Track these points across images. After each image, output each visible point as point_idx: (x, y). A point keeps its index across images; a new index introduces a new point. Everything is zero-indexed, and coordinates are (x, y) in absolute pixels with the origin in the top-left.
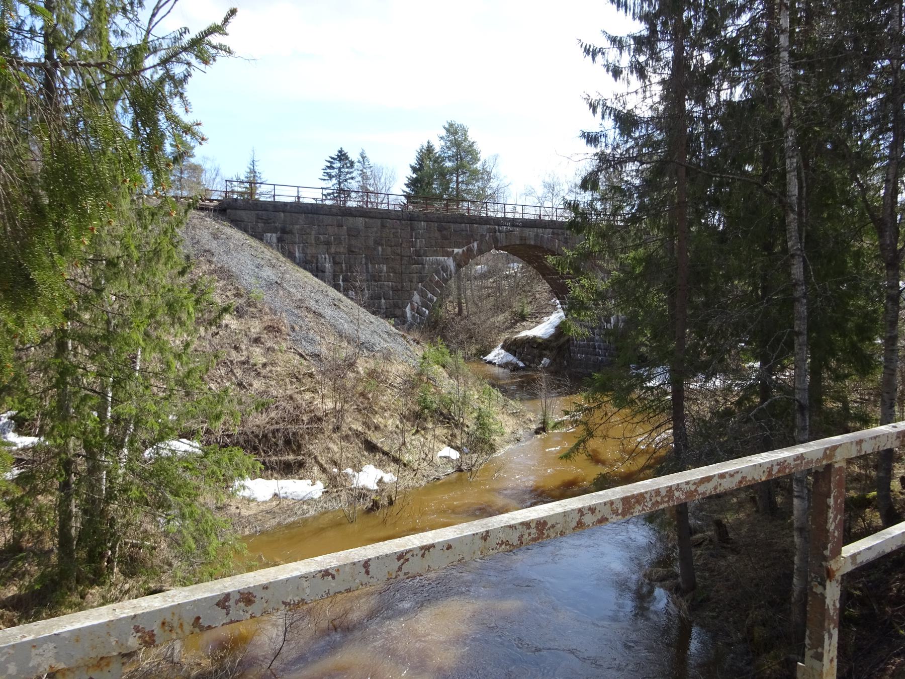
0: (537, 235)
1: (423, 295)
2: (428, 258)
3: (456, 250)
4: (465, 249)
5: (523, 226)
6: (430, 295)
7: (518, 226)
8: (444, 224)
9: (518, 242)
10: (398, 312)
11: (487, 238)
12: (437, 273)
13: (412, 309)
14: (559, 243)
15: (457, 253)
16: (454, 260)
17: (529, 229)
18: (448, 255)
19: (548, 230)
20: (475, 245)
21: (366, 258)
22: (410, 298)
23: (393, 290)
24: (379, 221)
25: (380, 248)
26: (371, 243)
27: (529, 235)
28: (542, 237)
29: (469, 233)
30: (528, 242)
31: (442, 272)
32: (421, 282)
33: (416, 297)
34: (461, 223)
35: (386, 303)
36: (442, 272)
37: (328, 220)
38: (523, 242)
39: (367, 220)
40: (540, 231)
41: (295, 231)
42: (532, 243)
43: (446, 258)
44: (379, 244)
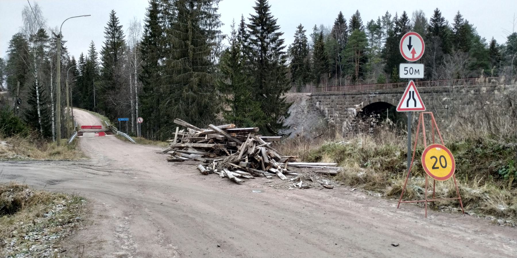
0: (385, 98)
1: (347, 123)
3: (357, 106)
5: (379, 94)
8: (353, 96)
9: (378, 101)
13: (344, 128)
16: (356, 110)
17: (382, 95)
18: (355, 107)
19: (389, 94)
20: (362, 103)
30: (381, 101)
32: (347, 118)
37: (327, 97)
40: (386, 95)
42: (383, 101)
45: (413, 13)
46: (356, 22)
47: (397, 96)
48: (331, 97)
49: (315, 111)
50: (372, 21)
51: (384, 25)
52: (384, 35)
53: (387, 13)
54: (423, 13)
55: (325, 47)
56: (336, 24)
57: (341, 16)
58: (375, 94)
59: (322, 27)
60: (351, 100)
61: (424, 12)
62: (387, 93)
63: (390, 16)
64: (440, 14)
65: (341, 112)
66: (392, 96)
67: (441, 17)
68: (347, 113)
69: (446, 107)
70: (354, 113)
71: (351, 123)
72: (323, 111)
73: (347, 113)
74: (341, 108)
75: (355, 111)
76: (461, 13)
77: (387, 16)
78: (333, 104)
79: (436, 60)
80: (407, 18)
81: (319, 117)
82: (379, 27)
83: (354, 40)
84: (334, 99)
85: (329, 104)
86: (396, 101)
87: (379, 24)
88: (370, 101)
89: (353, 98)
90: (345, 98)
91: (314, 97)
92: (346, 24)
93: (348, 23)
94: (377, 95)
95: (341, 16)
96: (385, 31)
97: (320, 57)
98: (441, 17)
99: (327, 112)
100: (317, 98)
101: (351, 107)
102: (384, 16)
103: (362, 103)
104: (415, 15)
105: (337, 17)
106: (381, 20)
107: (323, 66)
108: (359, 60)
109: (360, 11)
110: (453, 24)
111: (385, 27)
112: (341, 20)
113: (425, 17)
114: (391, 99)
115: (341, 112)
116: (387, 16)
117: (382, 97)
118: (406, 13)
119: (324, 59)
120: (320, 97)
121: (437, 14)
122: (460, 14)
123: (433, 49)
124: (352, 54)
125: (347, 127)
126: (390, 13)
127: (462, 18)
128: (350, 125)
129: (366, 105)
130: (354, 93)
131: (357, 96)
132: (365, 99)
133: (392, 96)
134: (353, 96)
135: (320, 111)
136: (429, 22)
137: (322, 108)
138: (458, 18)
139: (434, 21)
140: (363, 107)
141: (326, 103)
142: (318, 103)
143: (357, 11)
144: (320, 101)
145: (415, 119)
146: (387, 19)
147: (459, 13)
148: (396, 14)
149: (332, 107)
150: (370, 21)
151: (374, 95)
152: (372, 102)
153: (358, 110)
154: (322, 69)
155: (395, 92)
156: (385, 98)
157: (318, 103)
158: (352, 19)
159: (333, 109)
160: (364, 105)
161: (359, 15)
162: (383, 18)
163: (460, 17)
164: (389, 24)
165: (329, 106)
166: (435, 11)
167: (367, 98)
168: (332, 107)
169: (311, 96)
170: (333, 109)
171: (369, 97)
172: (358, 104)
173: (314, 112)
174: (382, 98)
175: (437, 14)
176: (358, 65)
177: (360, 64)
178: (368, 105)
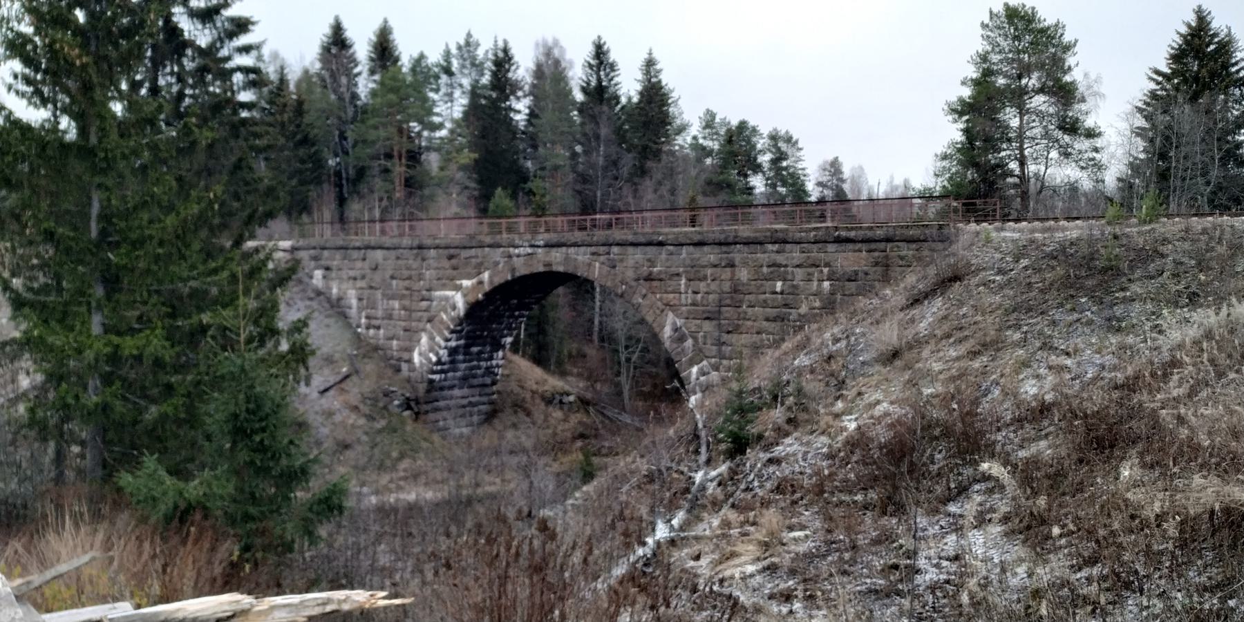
0: (567, 259)
1: (432, 338)
2: (438, 293)
3: (466, 283)
4: (474, 281)
5: (546, 246)
6: (438, 339)
7: (538, 247)
8: (452, 251)
9: (541, 269)
10: (405, 356)
11: (501, 266)
12: (446, 312)
13: (420, 354)
14: (600, 268)
15: (467, 288)
16: (465, 296)
17: (555, 249)
18: (458, 288)
19: (582, 249)
20: (486, 276)
21: (383, 295)
22: (419, 341)
23: (406, 330)
24: (393, 253)
25: (394, 282)
26: (387, 276)
27: (556, 258)
28: (576, 259)
29: (479, 260)
30: (555, 268)
31: (449, 310)
32: (429, 321)
33: (424, 339)
34: (471, 248)
35: (398, 345)
36: (449, 310)
37: (355, 254)
38: (547, 269)
39: (385, 252)
40: (572, 250)
41: (334, 268)
42: (561, 269)
43: (454, 293)
44: (392, 277)
45: (537, 45)
46: (384, 50)
47: (608, 253)
48: (370, 253)
49: (311, 299)
50: (422, 57)
51: (463, 66)
52: (464, 93)
53: (469, 35)
54: (561, 47)
55: (306, 107)
56: (326, 49)
57: (338, 29)
58: (532, 246)
59: (275, 56)
60: (446, 264)
61: (563, 43)
62: (575, 245)
63: (478, 45)
64: (608, 51)
65: (406, 302)
66: (593, 254)
67: (611, 60)
68: (429, 307)
69: (778, 289)
70: (454, 308)
71: (447, 340)
72: (340, 299)
73: (429, 307)
74: (407, 289)
75: (460, 301)
76: (656, 55)
77: (469, 45)
78: (377, 277)
79: (605, 169)
80: (510, 59)
81: (327, 321)
82: (448, 71)
83: (392, 97)
84: (380, 261)
85: (363, 277)
86: (606, 269)
87: (449, 63)
88: (513, 270)
89: (451, 257)
90: (424, 260)
91: (303, 255)
92: (353, 54)
93: (362, 49)
94: (540, 250)
95: (338, 29)
96: (466, 82)
97: (295, 134)
98: (611, 60)
99: (354, 302)
100: (316, 258)
101: (444, 287)
102: (462, 42)
103: (486, 276)
104: (541, 50)
105: (328, 30)
106: (454, 51)
107: (303, 162)
108: (404, 154)
109: (392, 23)
110: (639, 81)
111: (466, 71)
112: (338, 42)
113: (569, 55)
114: (589, 265)
115: (406, 302)
116: (468, 44)
117: (557, 256)
118: (511, 45)
119: (306, 141)
120: (326, 253)
121: (600, 52)
122: (654, 55)
123: (597, 137)
124: (381, 135)
125: (431, 350)
126: (476, 36)
127: (658, 67)
128: (443, 343)
129: (498, 280)
130: (456, 243)
131: (465, 254)
132: (497, 264)
133: (593, 254)
134: (452, 251)
135: (329, 300)
136: (577, 74)
137: (335, 291)
138: (650, 63)
139: (591, 66)
140: (487, 288)
141: (352, 273)
142: (318, 274)
143: (386, 21)
144: (328, 269)
145: (674, 323)
146: (469, 51)
147: (650, 54)
148: (496, 41)
149: (371, 288)
150: (416, 55)
151: (529, 250)
152: (523, 271)
153: (471, 299)
154: (300, 172)
155: (603, 240)
156: (567, 259)
157: (318, 274)
158: (374, 39)
159: (379, 294)
160: (491, 281)
161: (390, 33)
162: (459, 48)
163: (654, 64)
164: (477, 66)
165: (360, 284)
166: (594, 43)
167: (502, 261)
168: (371, 288)
169: (294, 249)
170: (379, 294)
171: (510, 257)
172: (469, 277)
173: (308, 303)
174: (557, 260)
175: (600, 52)
176: (404, 168)
177: (408, 167)
178: (507, 283)
